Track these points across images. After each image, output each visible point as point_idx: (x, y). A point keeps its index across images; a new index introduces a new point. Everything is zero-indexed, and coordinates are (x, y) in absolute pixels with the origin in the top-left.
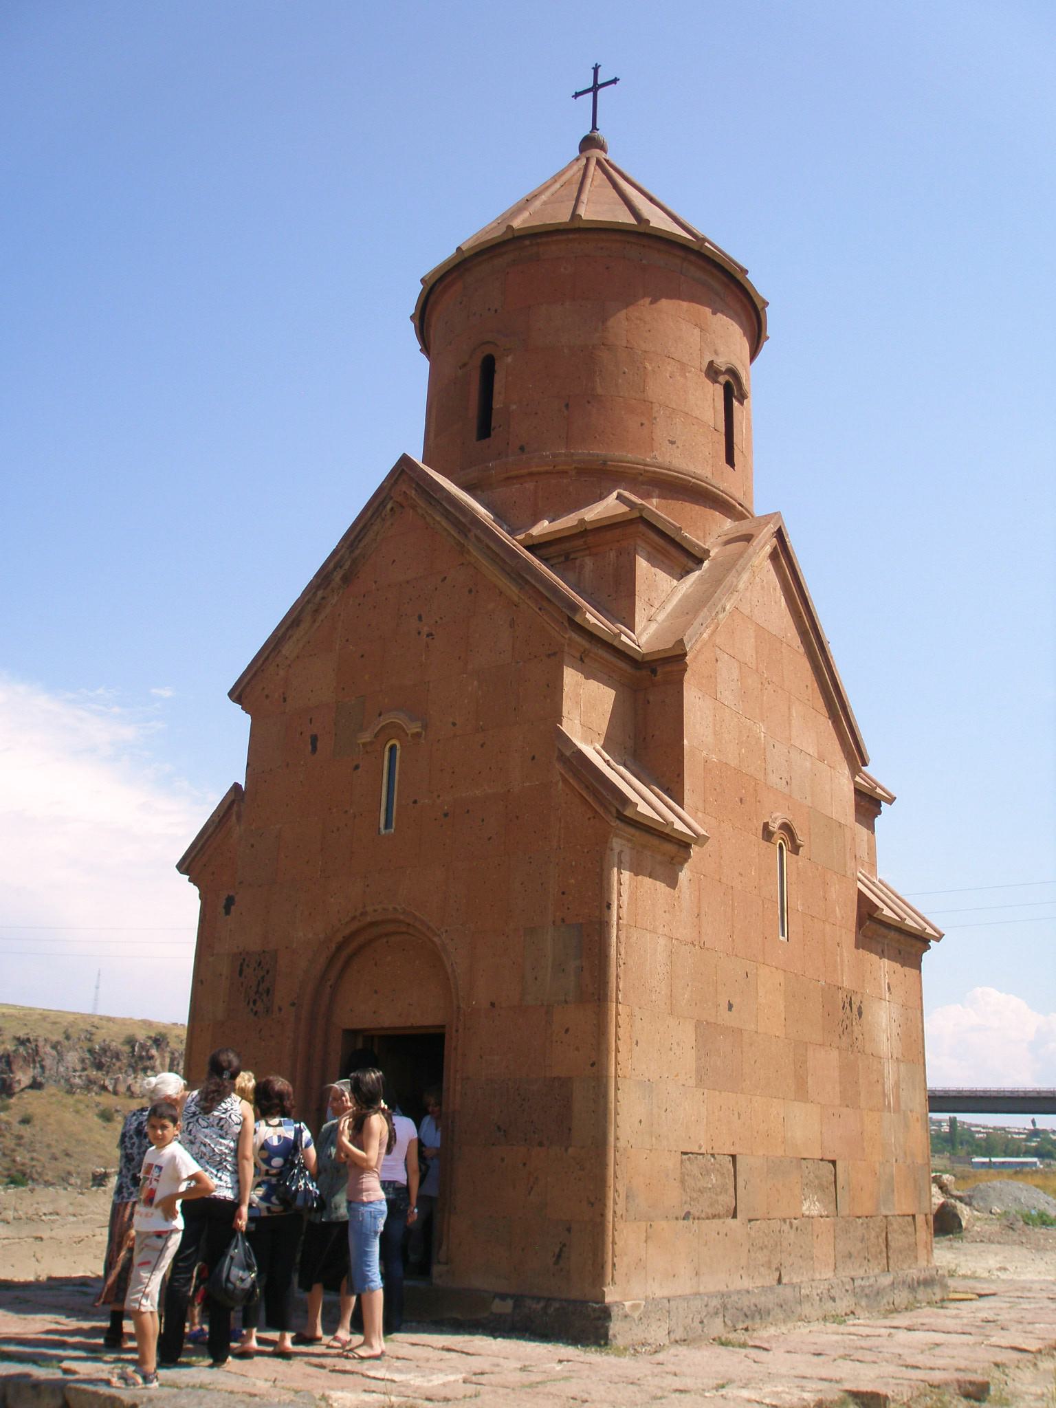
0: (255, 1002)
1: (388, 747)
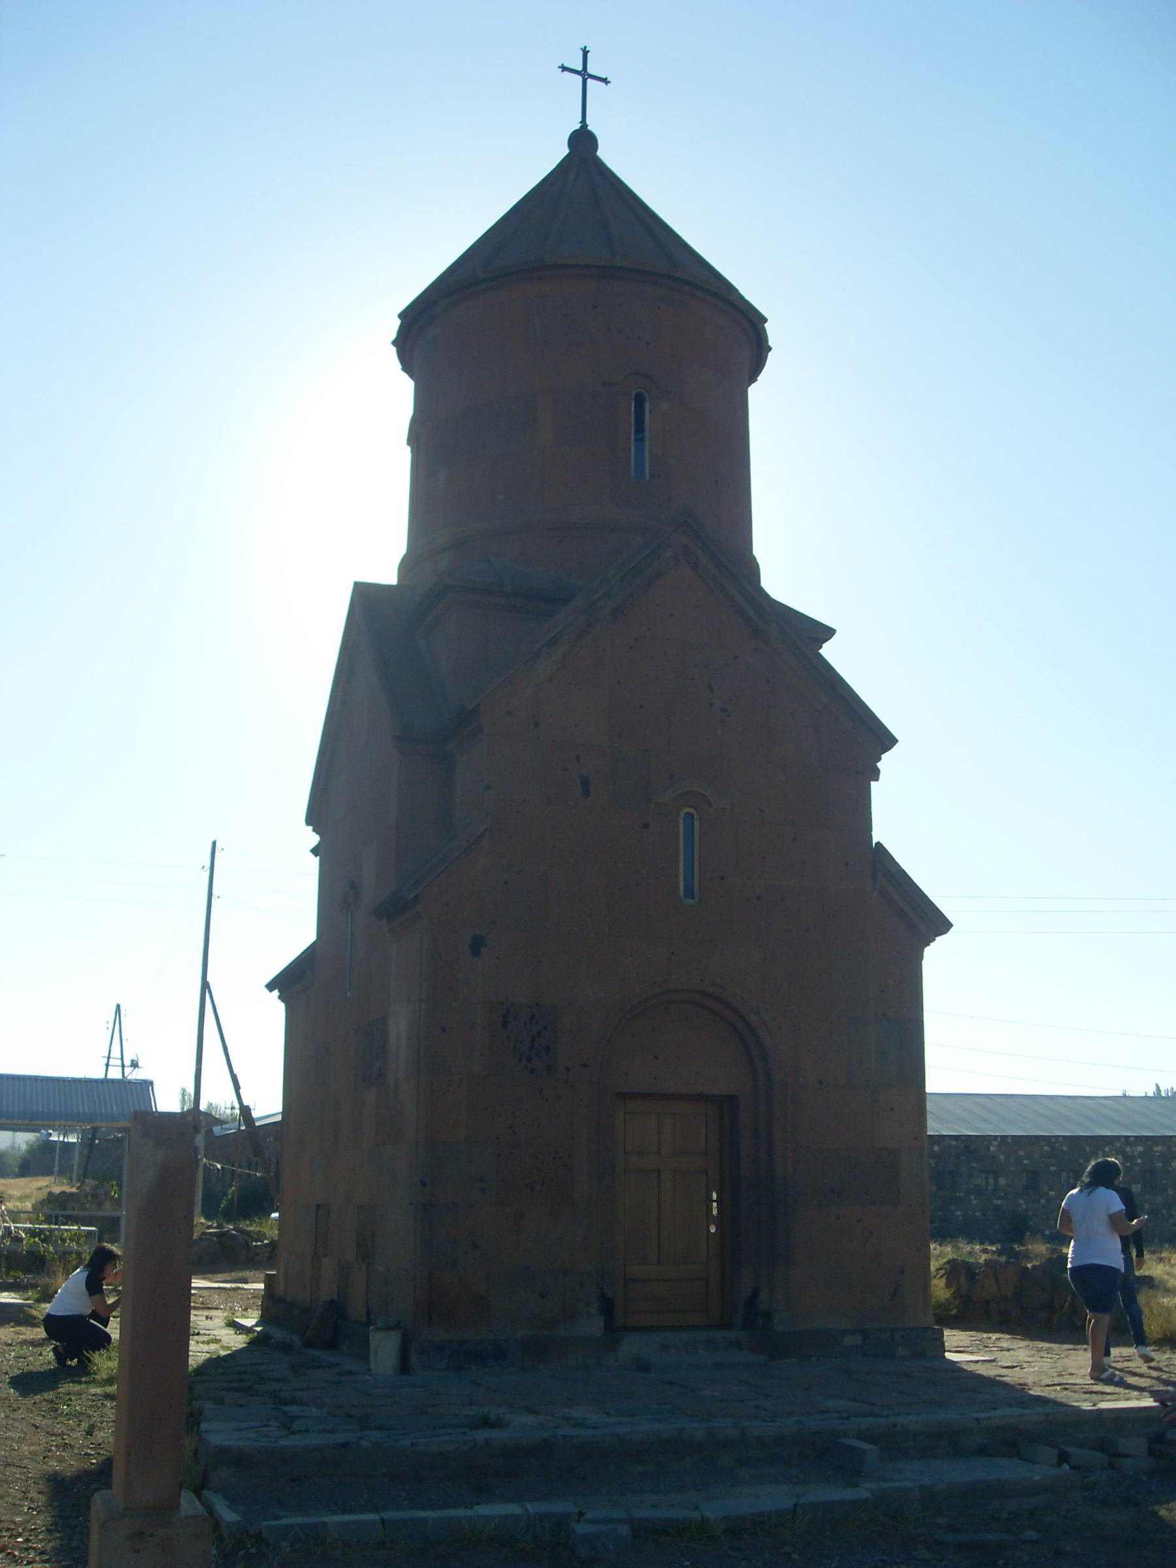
0: (529, 1059)
1: (682, 815)
